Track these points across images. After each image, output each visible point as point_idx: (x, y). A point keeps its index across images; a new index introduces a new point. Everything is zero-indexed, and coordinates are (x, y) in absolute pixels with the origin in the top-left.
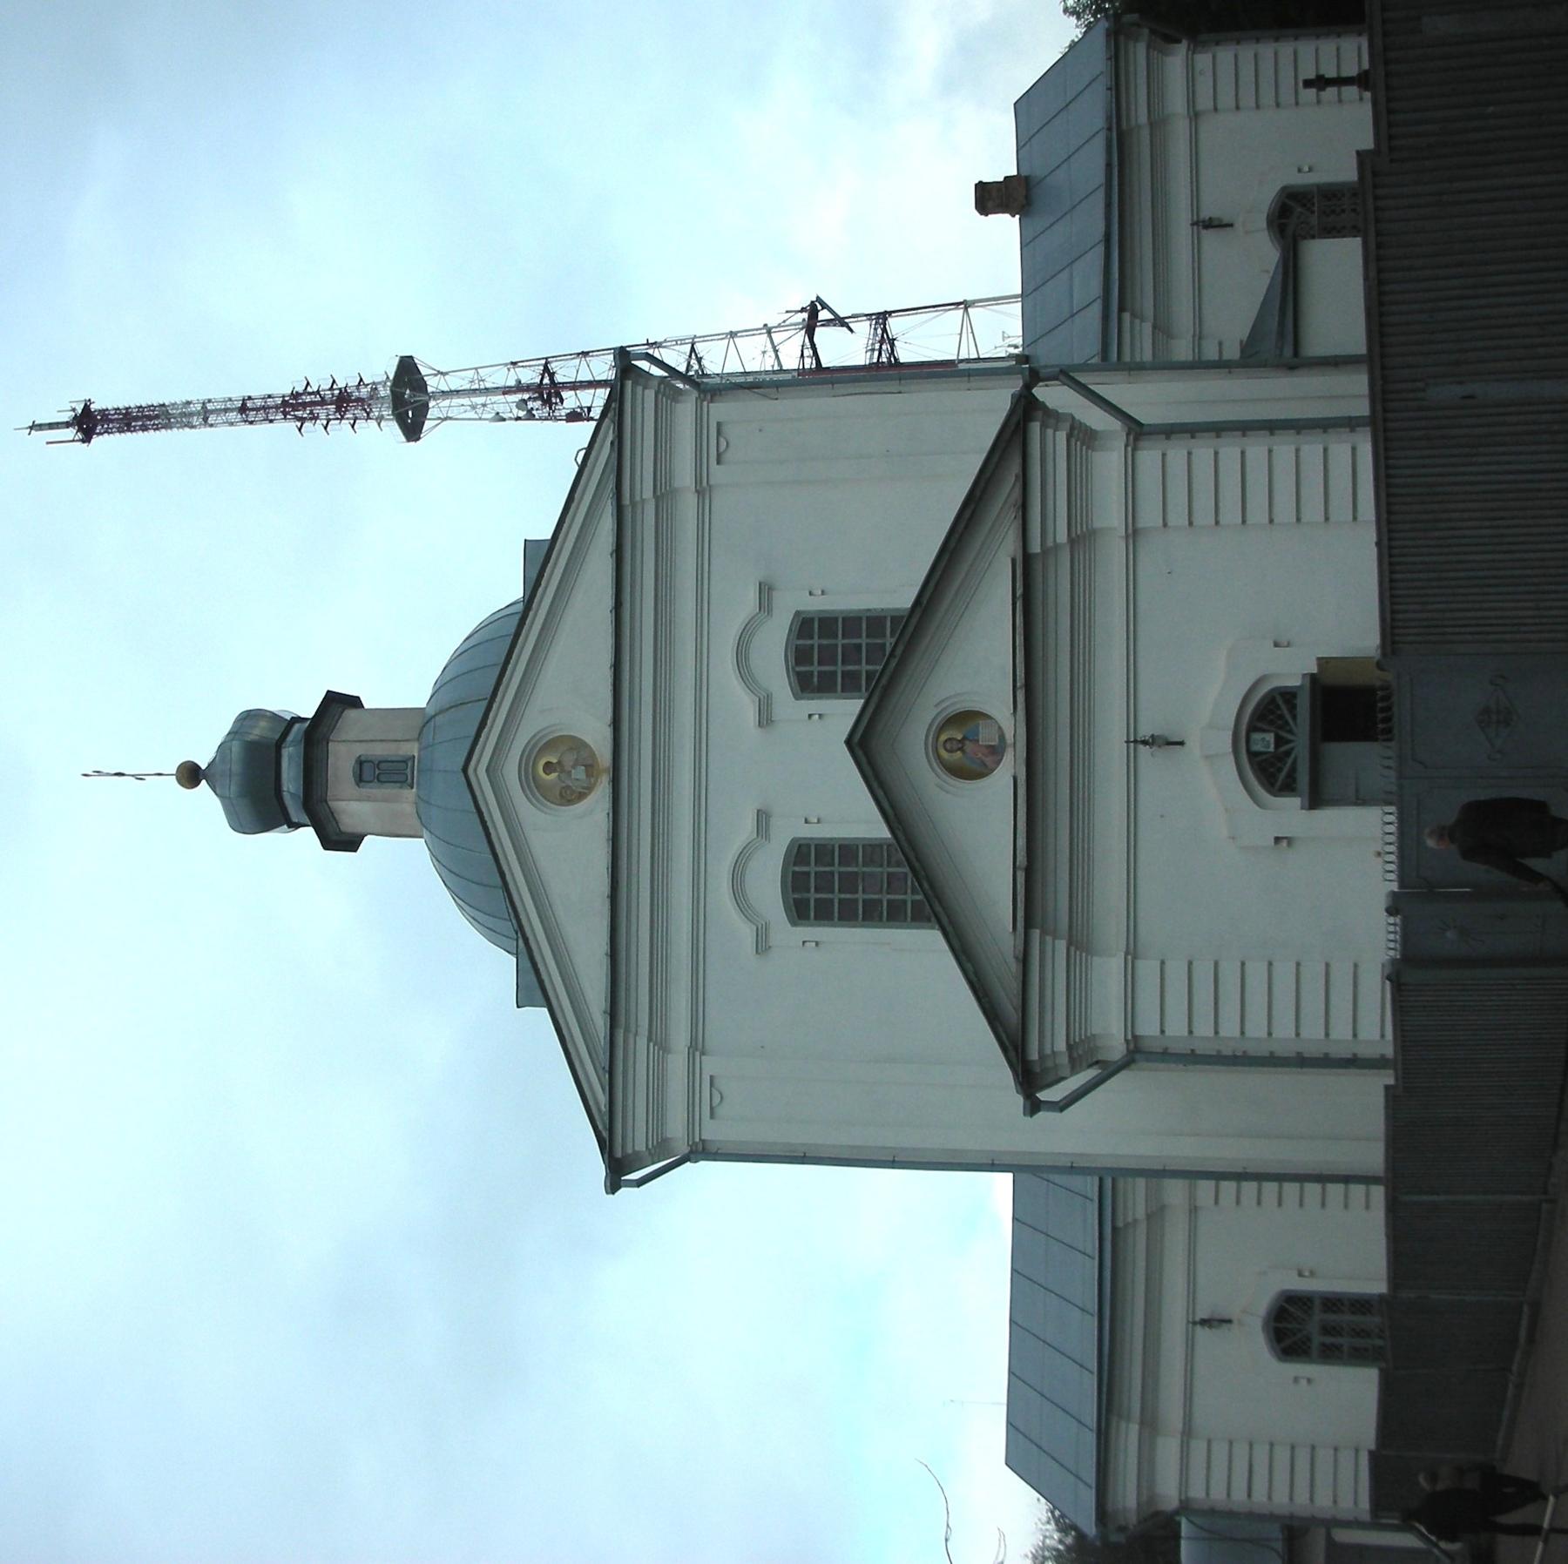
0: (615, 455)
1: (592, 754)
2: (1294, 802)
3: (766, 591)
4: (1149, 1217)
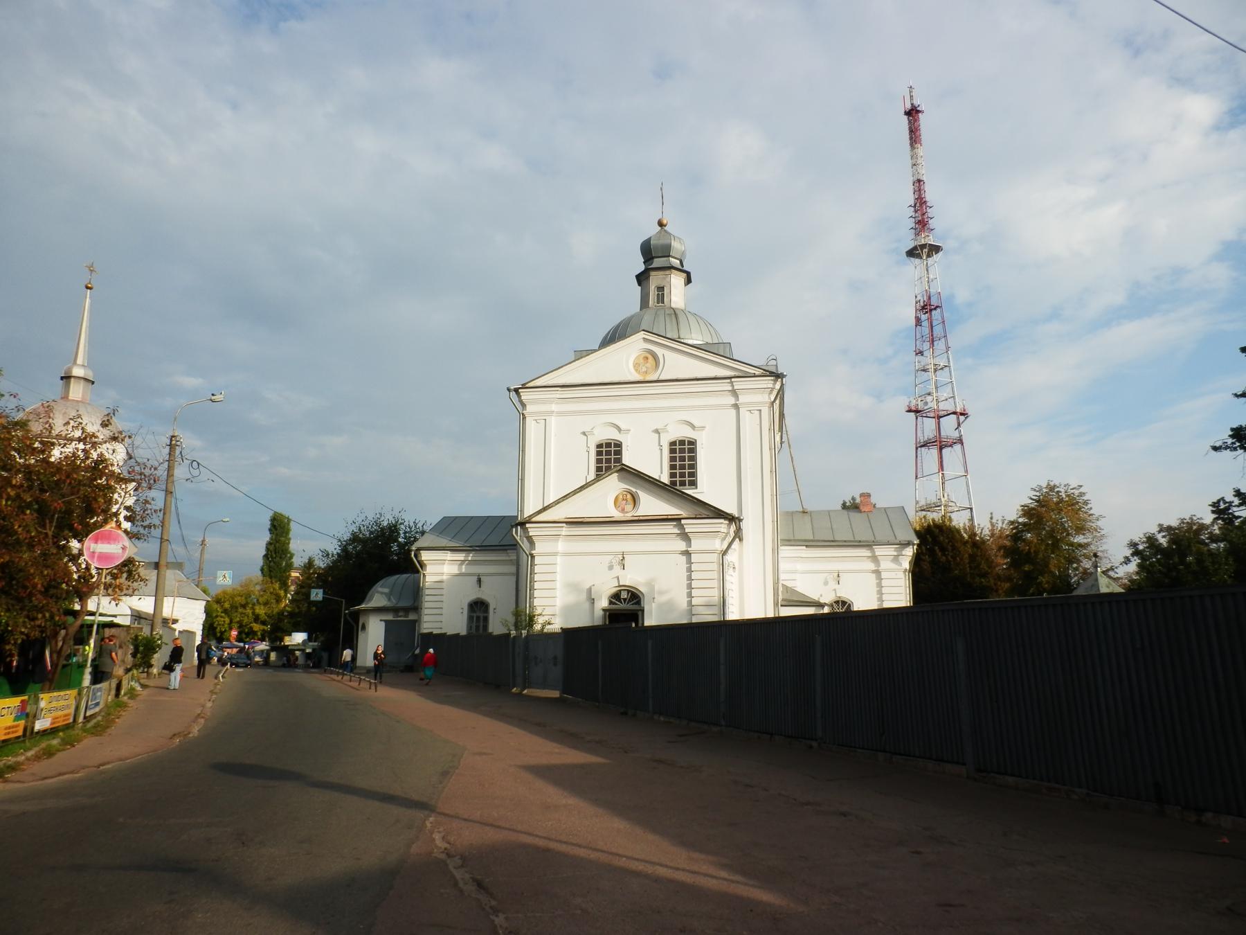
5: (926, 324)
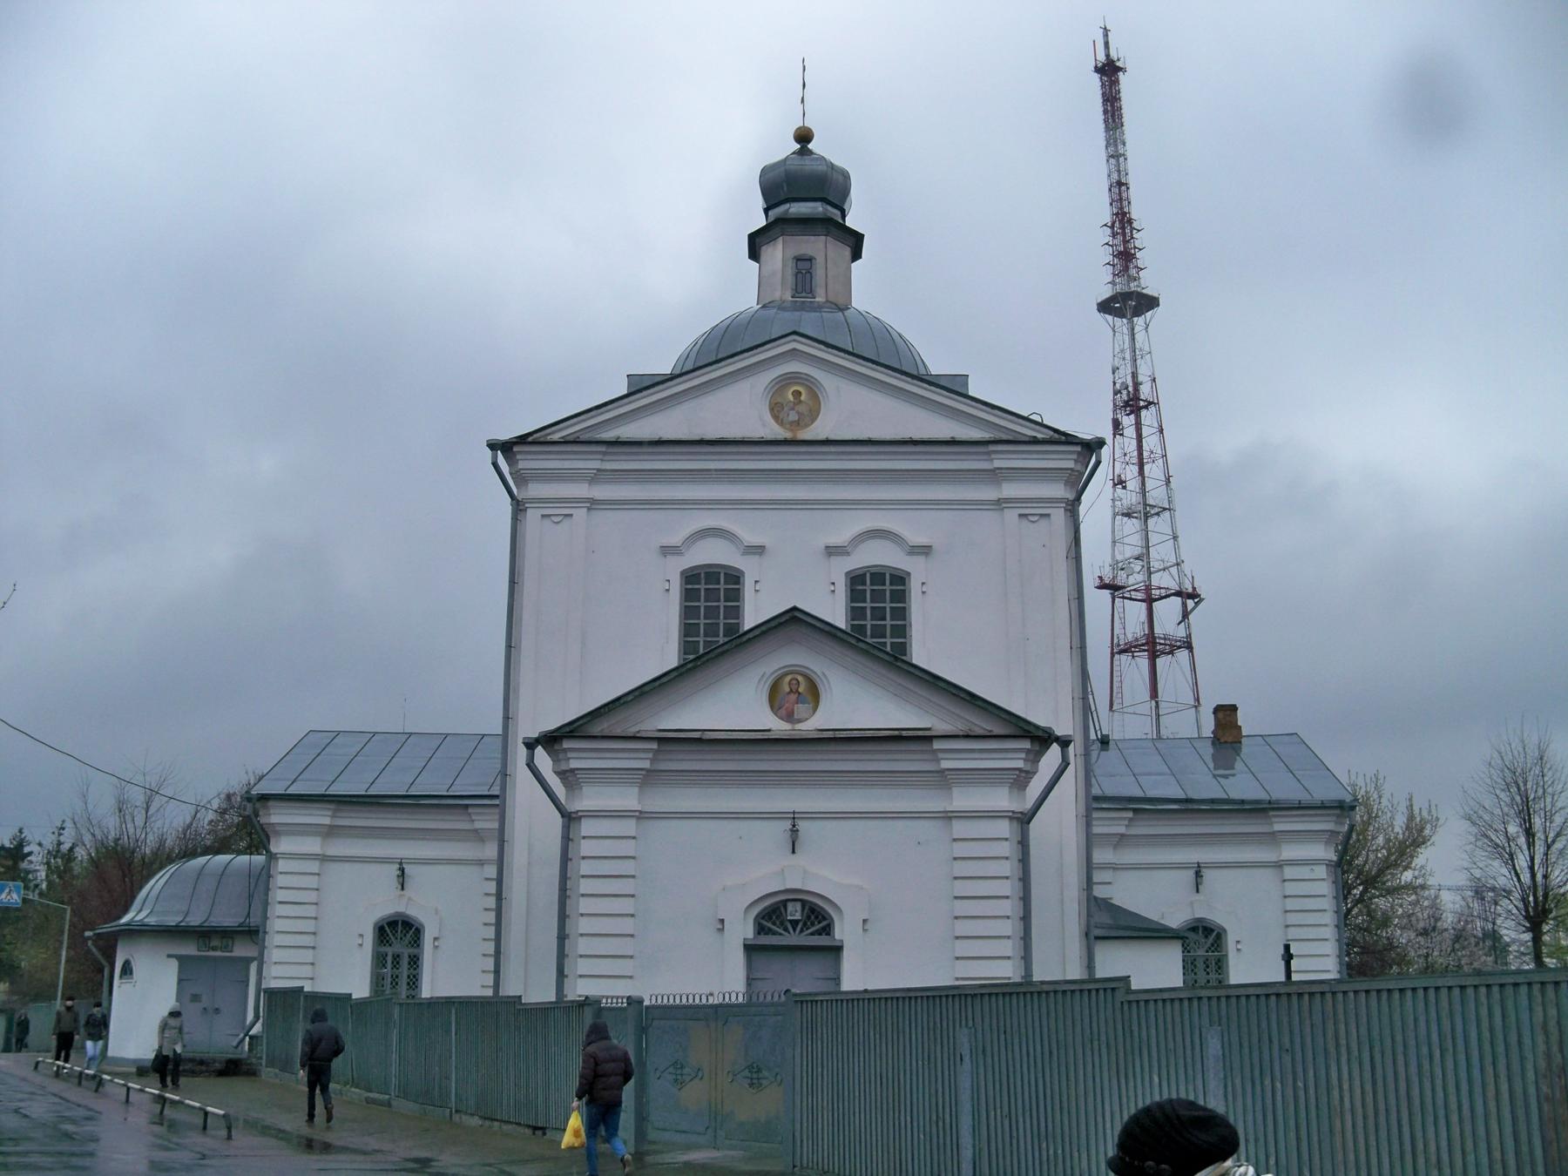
0: (1027, 439)
1: (807, 426)
2: (749, 932)
3: (925, 550)
4: (476, 831)
5: (1130, 432)
